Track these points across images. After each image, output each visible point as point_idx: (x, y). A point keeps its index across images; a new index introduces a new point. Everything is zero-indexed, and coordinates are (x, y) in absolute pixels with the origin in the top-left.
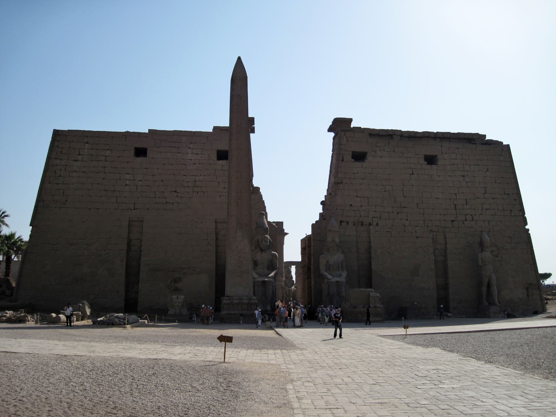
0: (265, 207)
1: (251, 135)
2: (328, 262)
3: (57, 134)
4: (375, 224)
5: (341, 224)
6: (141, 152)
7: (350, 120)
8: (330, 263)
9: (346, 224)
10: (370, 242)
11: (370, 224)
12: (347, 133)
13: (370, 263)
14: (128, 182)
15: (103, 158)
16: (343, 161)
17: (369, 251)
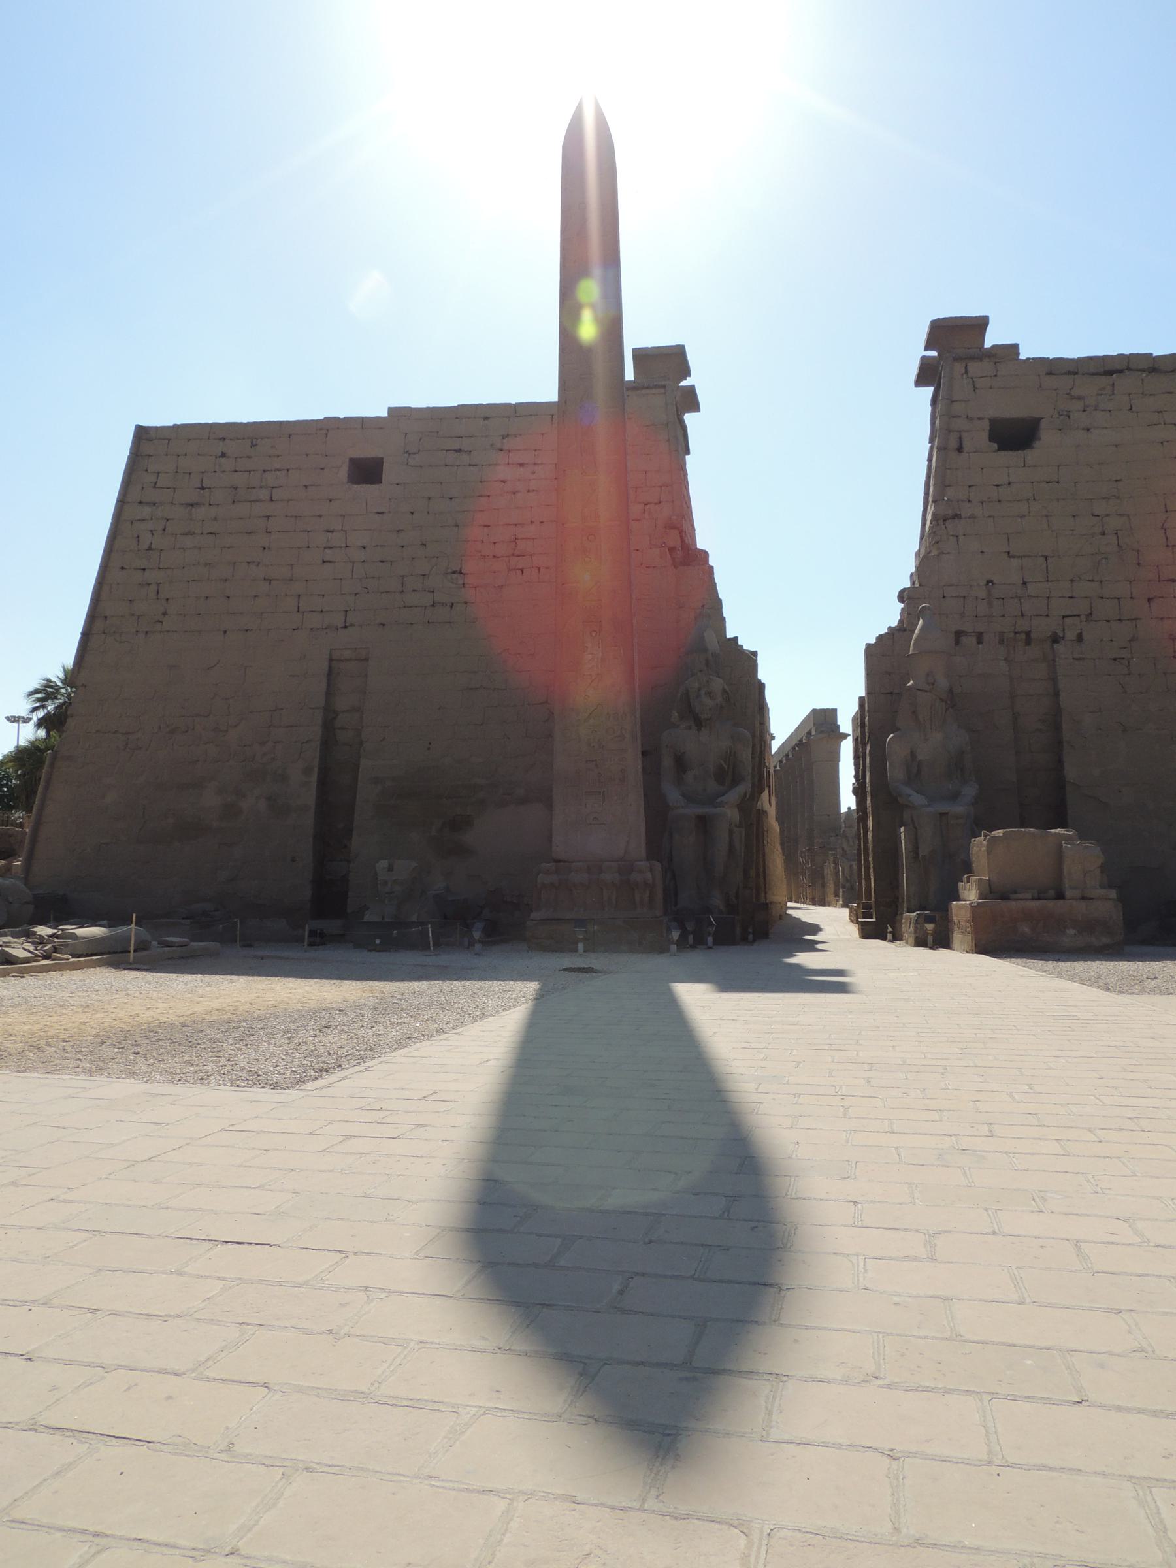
0: (720, 602)
1: (689, 418)
2: (913, 754)
3: (142, 435)
4: (1071, 635)
5: (957, 643)
6: (367, 472)
7: (980, 325)
8: (920, 757)
9: (974, 640)
10: (1057, 694)
11: (1055, 639)
12: (975, 368)
13: (1060, 761)
14: (329, 554)
15: (264, 494)
16: (960, 449)
17: (1055, 720)
